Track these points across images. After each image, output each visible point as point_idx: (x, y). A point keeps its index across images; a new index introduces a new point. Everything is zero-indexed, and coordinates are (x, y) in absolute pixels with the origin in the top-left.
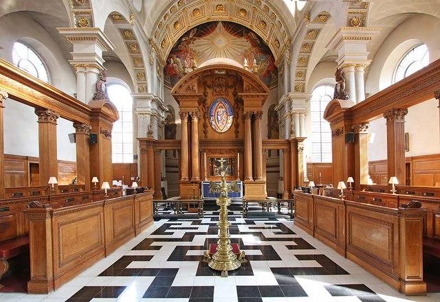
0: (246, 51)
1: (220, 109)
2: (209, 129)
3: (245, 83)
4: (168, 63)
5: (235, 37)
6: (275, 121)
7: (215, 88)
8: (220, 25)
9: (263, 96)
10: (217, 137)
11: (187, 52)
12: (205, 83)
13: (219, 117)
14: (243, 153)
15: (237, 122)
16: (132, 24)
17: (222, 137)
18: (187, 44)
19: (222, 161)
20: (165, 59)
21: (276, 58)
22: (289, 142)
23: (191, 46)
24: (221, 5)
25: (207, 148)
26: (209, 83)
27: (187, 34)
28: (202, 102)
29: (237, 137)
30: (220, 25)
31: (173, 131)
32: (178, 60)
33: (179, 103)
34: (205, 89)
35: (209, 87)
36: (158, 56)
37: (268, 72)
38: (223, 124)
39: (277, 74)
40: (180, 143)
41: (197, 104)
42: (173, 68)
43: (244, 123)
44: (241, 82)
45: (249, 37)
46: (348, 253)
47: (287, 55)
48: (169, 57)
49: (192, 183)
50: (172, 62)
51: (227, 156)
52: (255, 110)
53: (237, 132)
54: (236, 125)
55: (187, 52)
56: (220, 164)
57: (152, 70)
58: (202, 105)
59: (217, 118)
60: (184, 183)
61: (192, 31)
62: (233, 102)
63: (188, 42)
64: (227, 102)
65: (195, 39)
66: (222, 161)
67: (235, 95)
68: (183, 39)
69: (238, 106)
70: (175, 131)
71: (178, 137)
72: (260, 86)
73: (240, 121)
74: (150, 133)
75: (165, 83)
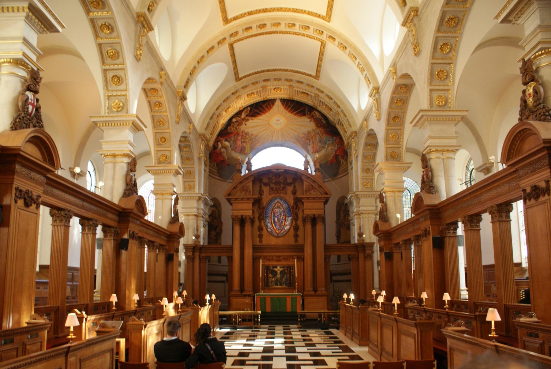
0: (309, 133)
1: (276, 210)
2: (264, 232)
3: (305, 184)
4: (215, 147)
5: (296, 117)
6: (345, 216)
7: (272, 186)
8: (278, 103)
9: (324, 197)
10: (273, 241)
11: (238, 134)
12: (260, 180)
13: (276, 219)
14: (301, 259)
15: (296, 223)
16: (190, 133)
17: (280, 242)
18: (238, 125)
19: (278, 269)
20: (211, 144)
21: (345, 141)
22: (356, 246)
23: (243, 128)
24: (278, 88)
25: (261, 254)
26: (265, 180)
27: (239, 114)
28: (257, 202)
29: (296, 241)
30: (278, 103)
31: (218, 230)
32: (227, 143)
33: (231, 204)
34: (261, 187)
35: (265, 185)
36: (207, 146)
37: (336, 157)
38: (280, 226)
39: (346, 160)
40: (230, 249)
41: (251, 205)
42: (221, 153)
43: (304, 226)
44: (302, 181)
45: (313, 116)
46: (354, 338)
47: (354, 145)
48: (217, 141)
49: (245, 296)
50: (220, 145)
51: (284, 263)
52: (317, 212)
53: (296, 236)
54: (296, 228)
55: (238, 134)
56: (276, 272)
57: (200, 164)
58: (256, 207)
59: (274, 220)
60: (237, 296)
61: (245, 111)
62: (292, 202)
63: (240, 124)
64: (285, 201)
65: (248, 120)
66: (278, 269)
67: (294, 192)
68: (234, 120)
69: (297, 206)
70: (221, 230)
71: (226, 240)
72: (321, 186)
73: (300, 222)
74: (197, 237)
75: (210, 171)
